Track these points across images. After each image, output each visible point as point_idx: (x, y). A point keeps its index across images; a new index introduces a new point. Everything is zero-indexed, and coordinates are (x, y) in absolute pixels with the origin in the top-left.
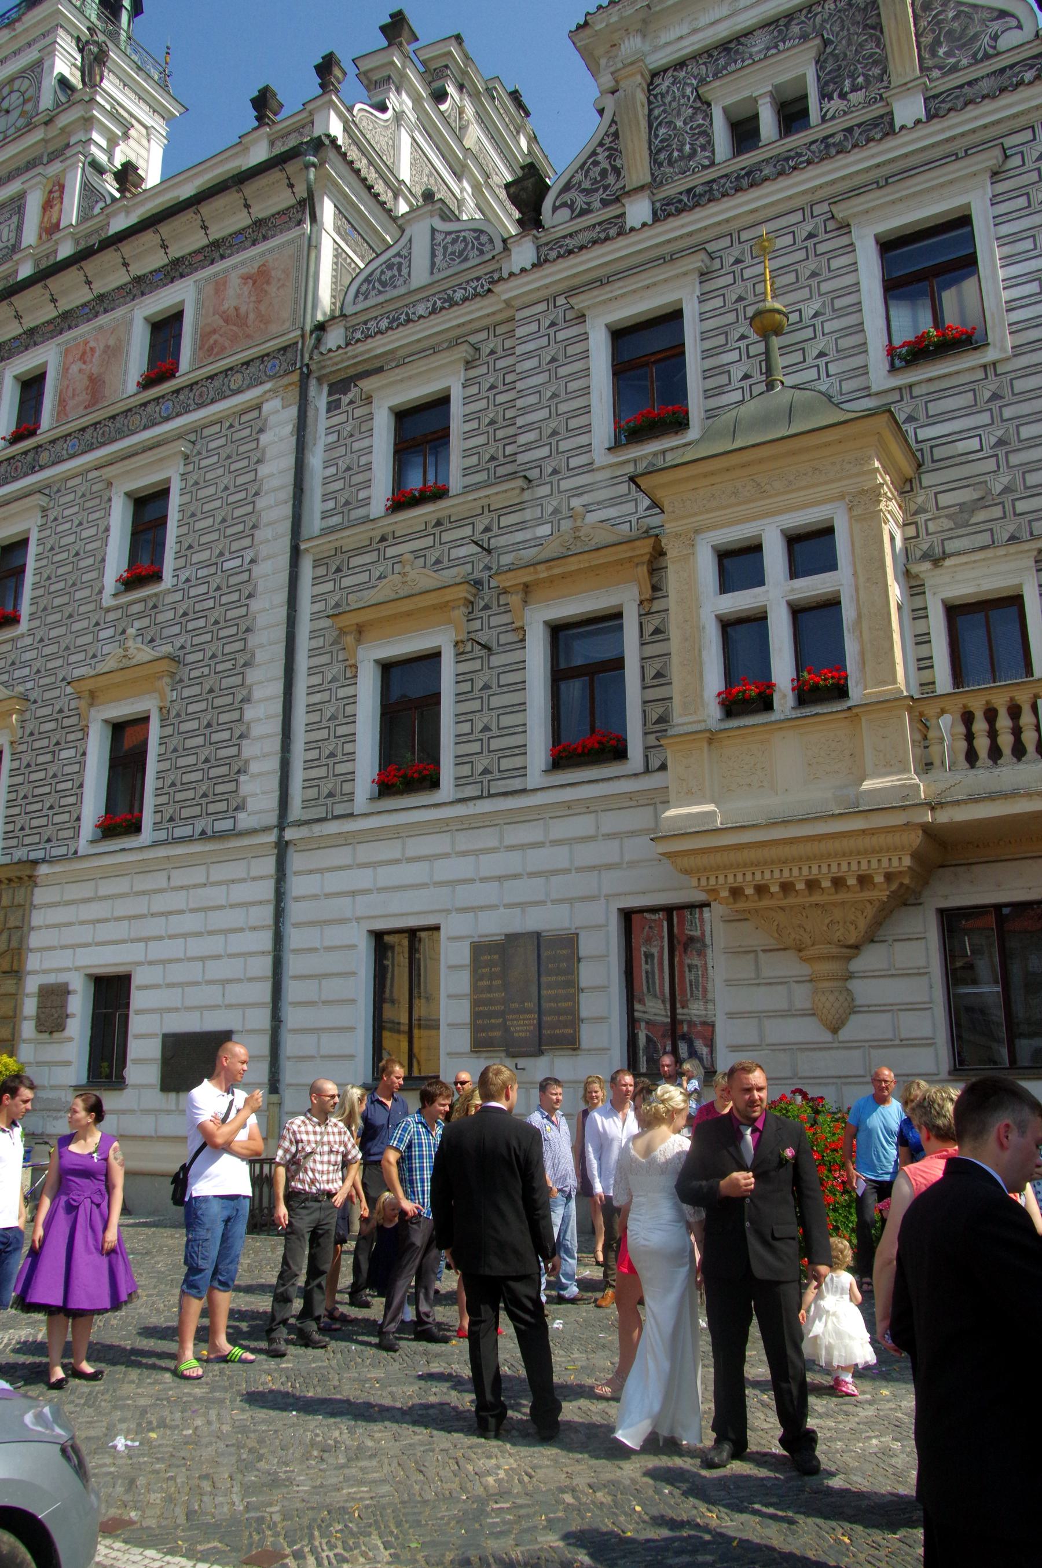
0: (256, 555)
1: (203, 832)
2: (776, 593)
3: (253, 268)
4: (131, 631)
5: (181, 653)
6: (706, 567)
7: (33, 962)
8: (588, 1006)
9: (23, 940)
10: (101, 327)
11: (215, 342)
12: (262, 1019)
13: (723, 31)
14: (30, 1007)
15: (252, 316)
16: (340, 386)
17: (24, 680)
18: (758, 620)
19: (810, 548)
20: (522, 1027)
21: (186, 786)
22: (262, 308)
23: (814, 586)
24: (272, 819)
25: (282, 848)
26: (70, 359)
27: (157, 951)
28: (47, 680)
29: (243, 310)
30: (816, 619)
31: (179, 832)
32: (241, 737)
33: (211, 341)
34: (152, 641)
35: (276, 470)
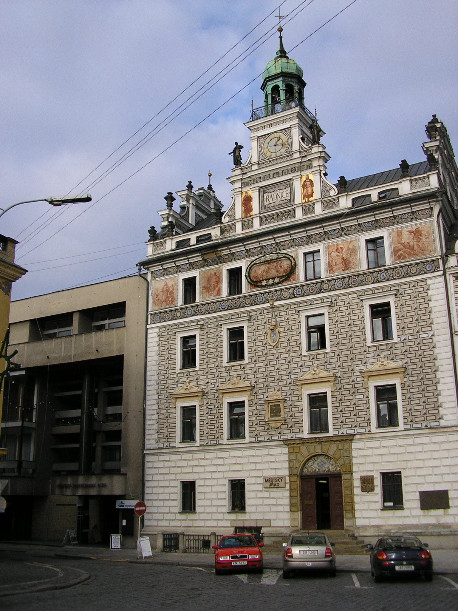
0: (434, 333)
1: (426, 426)
4: (382, 356)
5: (406, 365)
7: (355, 468)
9: (351, 461)
10: (344, 240)
11: (401, 254)
14: (357, 483)
15: (416, 247)
17: (333, 369)
21: (416, 411)
26: (331, 250)
27: (410, 465)
28: (345, 370)
29: (411, 244)
31: (415, 426)
32: (438, 395)
33: (399, 253)
34: (392, 359)
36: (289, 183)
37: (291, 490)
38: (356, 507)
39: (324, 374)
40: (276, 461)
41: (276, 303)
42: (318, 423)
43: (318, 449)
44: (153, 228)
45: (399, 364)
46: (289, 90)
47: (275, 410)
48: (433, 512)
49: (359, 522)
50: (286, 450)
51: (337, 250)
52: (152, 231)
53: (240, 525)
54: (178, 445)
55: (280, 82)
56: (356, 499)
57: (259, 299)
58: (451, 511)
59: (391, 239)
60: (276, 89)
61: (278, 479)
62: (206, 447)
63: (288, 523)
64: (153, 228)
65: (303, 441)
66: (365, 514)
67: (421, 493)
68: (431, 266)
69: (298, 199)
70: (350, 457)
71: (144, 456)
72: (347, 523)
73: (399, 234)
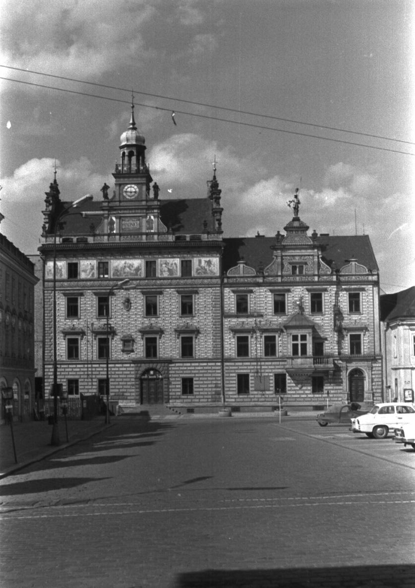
3: (207, 259)
15: (208, 270)
18: (297, 344)
19: (304, 338)
21: (202, 350)
22: (210, 268)
23: (303, 342)
25: (222, 362)
29: (206, 267)
30: (304, 347)
51: (166, 264)
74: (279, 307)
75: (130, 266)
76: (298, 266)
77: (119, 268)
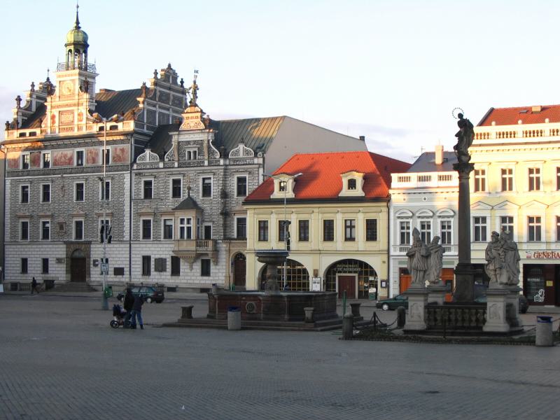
2: (185, 225)
6: (179, 221)
8: (167, 266)
12: (128, 266)
13: (188, 140)
14: (92, 263)
16: (136, 175)
18: (184, 228)
19: (189, 220)
20: (160, 269)
24: (129, 239)
35: (127, 186)
36: (72, 112)
37: (66, 264)
38: (92, 273)
39: (81, 212)
40: (60, 251)
41: (64, 175)
42: (79, 235)
43: (77, 247)
44: (8, 122)
45: (110, 211)
46: (77, 51)
47: (61, 228)
48: (118, 276)
49: (92, 279)
50: (65, 246)
52: (8, 124)
53: (46, 279)
54: (19, 241)
55: (72, 48)
56: (91, 269)
57: (57, 172)
58: (124, 276)
59: (112, 151)
60: (70, 51)
61: (61, 259)
62: (32, 243)
63: (65, 279)
64: (8, 122)
65: (72, 243)
66: (95, 276)
67: (115, 268)
68: (124, 168)
69: (76, 122)
70: (90, 251)
71: (4, 245)
72: (87, 279)
73: (116, 149)
74: (176, 193)
75: (65, 156)
76: (192, 151)
77: (57, 158)
